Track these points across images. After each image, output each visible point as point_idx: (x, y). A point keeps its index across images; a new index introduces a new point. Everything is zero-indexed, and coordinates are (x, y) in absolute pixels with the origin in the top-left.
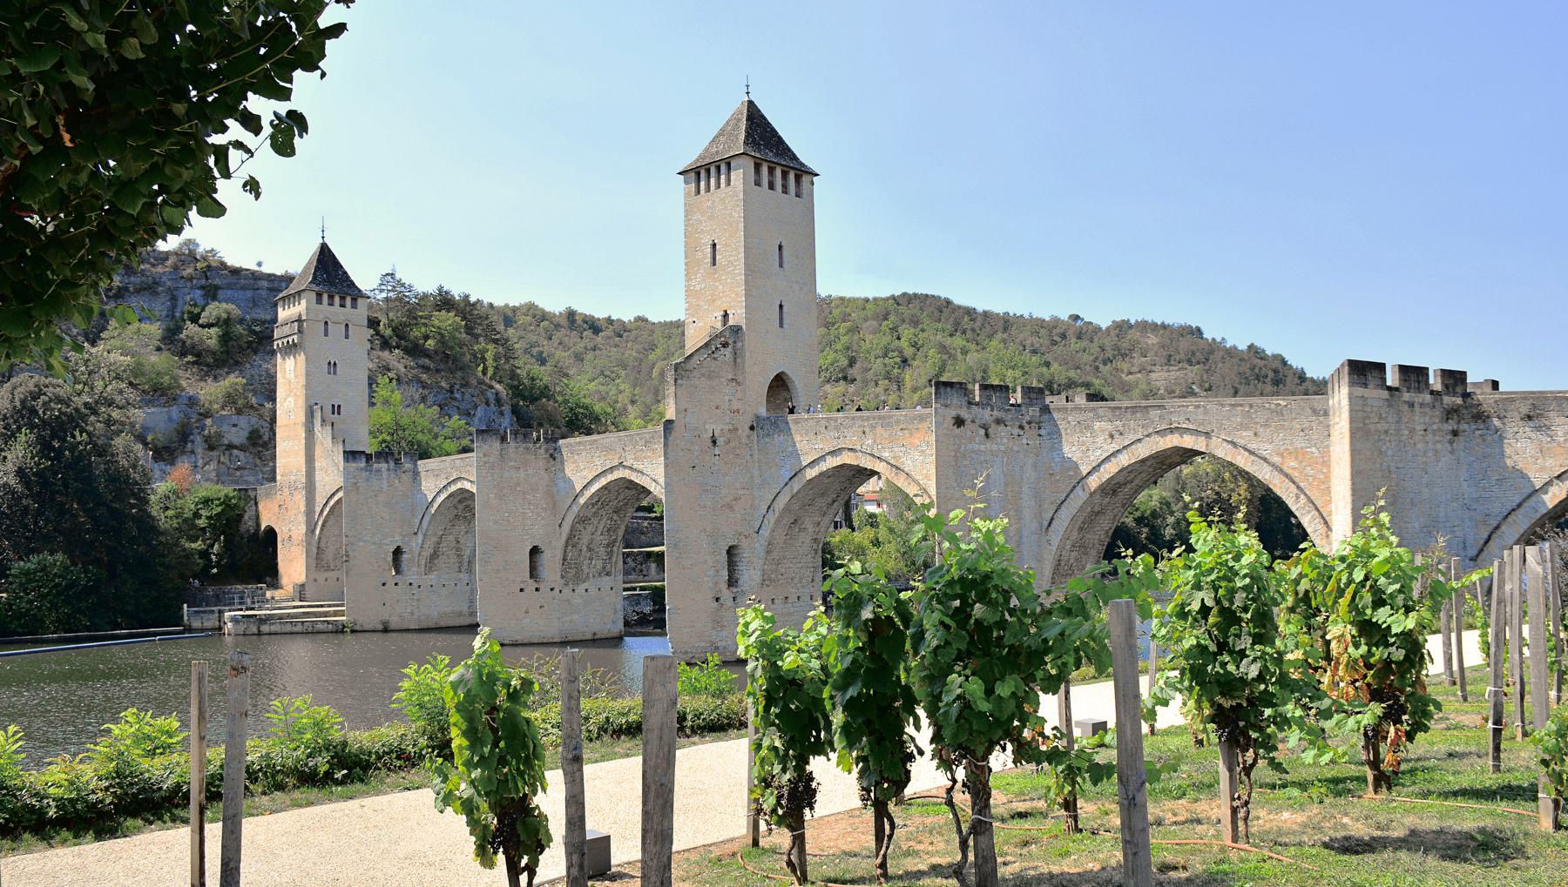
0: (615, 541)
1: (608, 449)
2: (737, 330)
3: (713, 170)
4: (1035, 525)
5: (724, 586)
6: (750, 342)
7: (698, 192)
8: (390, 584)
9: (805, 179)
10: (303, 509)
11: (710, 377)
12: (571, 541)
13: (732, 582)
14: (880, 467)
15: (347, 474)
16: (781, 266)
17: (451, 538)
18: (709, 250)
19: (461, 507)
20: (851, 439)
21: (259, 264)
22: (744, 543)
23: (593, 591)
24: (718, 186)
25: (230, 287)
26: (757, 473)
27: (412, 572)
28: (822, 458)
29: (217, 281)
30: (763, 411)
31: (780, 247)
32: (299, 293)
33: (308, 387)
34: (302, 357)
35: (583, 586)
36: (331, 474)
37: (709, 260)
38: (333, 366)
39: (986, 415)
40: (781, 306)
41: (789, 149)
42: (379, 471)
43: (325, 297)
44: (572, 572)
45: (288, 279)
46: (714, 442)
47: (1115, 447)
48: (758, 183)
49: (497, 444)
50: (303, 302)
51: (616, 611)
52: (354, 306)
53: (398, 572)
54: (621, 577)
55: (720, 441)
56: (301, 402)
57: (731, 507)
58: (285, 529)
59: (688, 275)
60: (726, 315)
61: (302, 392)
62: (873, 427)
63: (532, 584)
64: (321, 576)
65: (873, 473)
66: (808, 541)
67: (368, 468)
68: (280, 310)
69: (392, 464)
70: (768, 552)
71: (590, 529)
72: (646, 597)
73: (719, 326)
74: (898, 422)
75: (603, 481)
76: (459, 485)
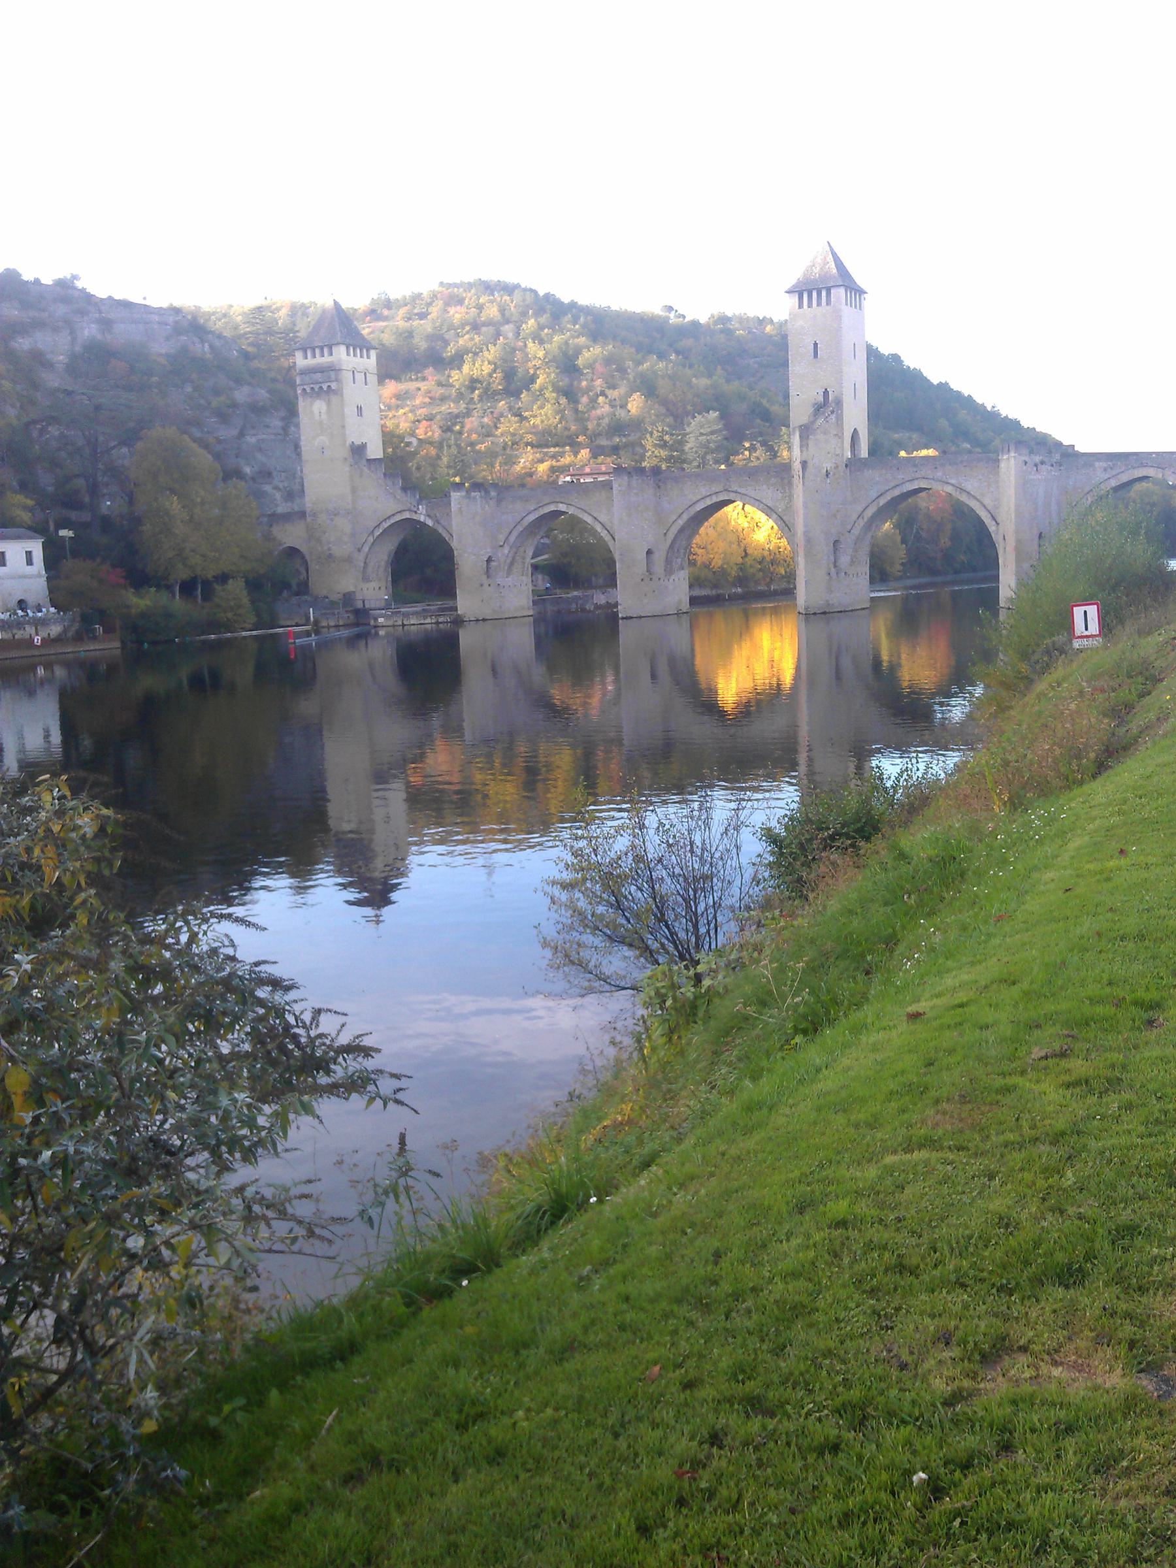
8: (486, 583)
11: (825, 433)
12: (671, 546)
22: (842, 539)
24: (819, 304)
29: (112, 316)
35: (673, 577)
38: (360, 409)
42: (475, 498)
47: (1107, 476)
52: (368, 357)
60: (826, 393)
62: (943, 465)
64: (365, 586)
74: (962, 462)
76: (552, 508)
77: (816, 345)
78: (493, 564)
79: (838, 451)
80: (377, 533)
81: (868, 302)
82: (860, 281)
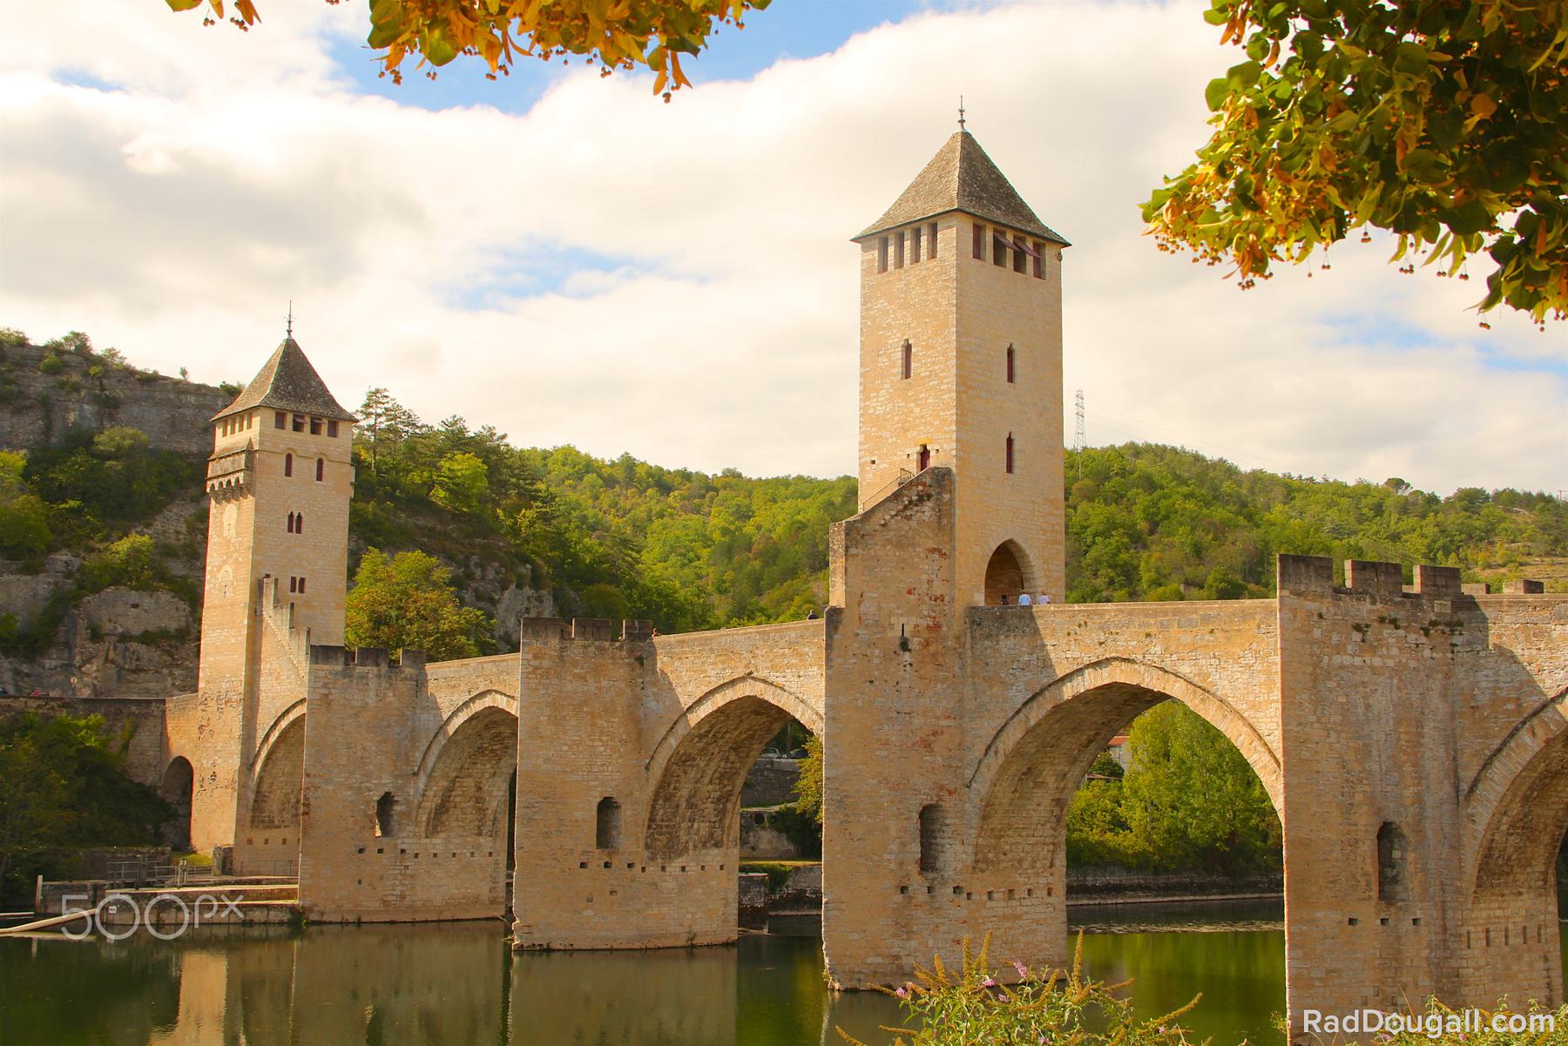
0: (730, 793)
1: (728, 653)
2: (943, 478)
3: (908, 234)
4: (1448, 789)
5: (914, 869)
6: (963, 491)
7: (884, 267)
9: (1049, 252)
10: (237, 730)
11: (899, 545)
12: (664, 791)
13: (927, 863)
14: (1175, 689)
15: (314, 677)
16: (1011, 378)
17: (470, 782)
18: (898, 355)
19: (488, 735)
20: (1125, 644)
21: (184, 373)
22: (948, 803)
23: (693, 868)
25: (137, 401)
26: (968, 692)
27: (409, 837)
28: (1079, 671)
29: (119, 393)
30: (980, 599)
31: (1010, 353)
32: (250, 412)
33: (257, 549)
34: (249, 502)
36: (288, 679)
37: (899, 369)
38: (295, 524)
39: (1365, 610)
40: (1010, 441)
41: (1022, 204)
42: (363, 677)
43: (289, 418)
44: (664, 841)
45: (232, 393)
46: (904, 645)
48: (977, 255)
49: (554, 642)
50: (256, 421)
51: (726, 905)
52: (333, 432)
53: (386, 831)
54: (736, 851)
55: (915, 644)
56: (245, 573)
57: (927, 745)
58: (207, 763)
59: (866, 391)
60: (924, 454)
61: (246, 558)
62: (1164, 627)
63: (599, 857)
64: (259, 836)
65: (1161, 697)
66: (1046, 802)
67: (346, 673)
68: (219, 432)
69: (384, 668)
70: (985, 818)
71: (692, 774)
72: (762, 882)
73: (913, 468)
75: (720, 700)
77: (908, 349)
78: (397, 808)
79: (939, 588)
80: (273, 739)
81: (1072, 268)
82: (1049, 215)
